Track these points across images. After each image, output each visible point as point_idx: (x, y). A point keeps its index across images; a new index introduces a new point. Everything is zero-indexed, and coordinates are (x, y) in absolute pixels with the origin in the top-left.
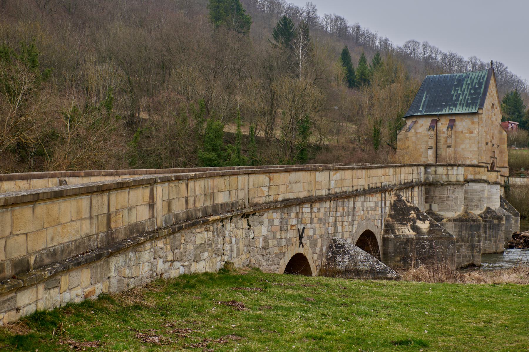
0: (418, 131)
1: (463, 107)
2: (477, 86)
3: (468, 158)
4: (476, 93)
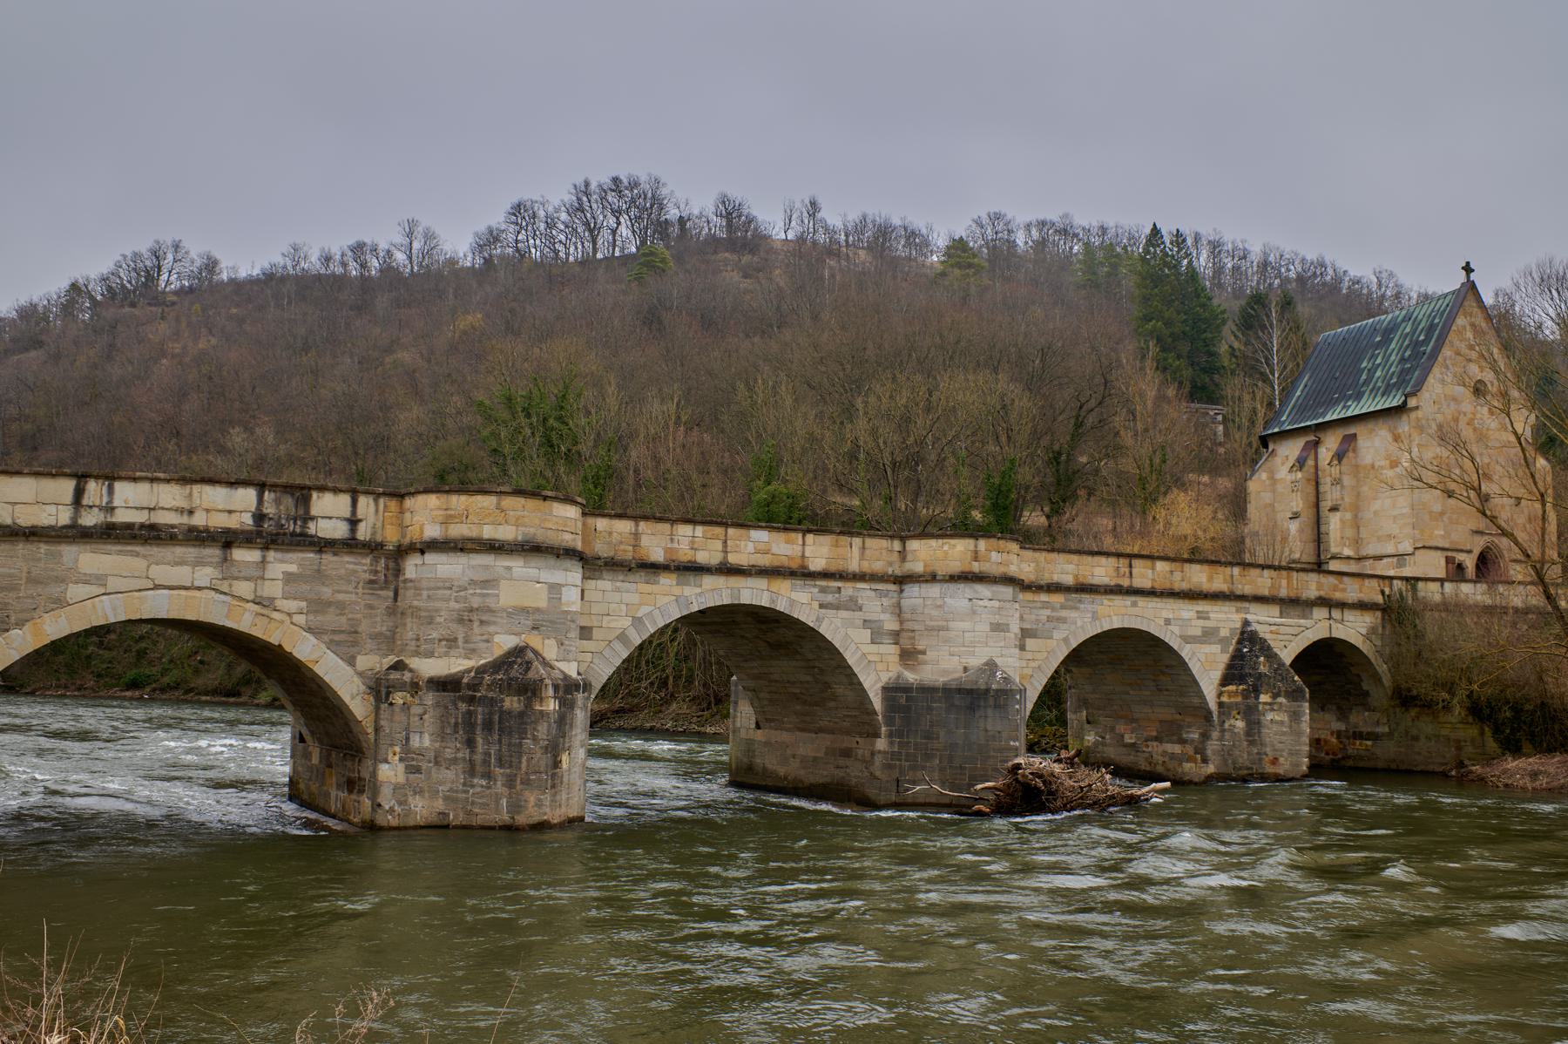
3: (1390, 536)
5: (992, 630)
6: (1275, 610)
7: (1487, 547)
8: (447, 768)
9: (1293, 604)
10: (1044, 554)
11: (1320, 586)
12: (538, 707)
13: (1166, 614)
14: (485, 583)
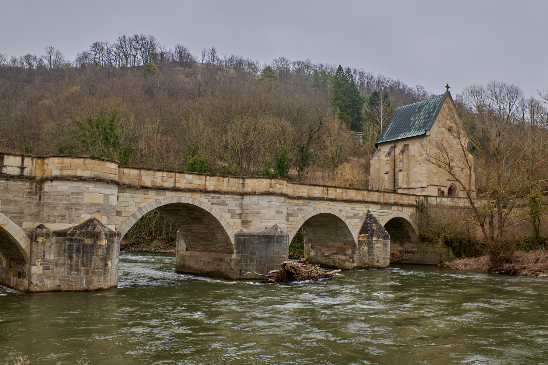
5: (277, 213)
6: (379, 207)
7: (452, 185)
8: (61, 268)
9: (385, 205)
10: (296, 185)
11: (395, 198)
12: (99, 243)
13: (340, 208)
14: (78, 194)
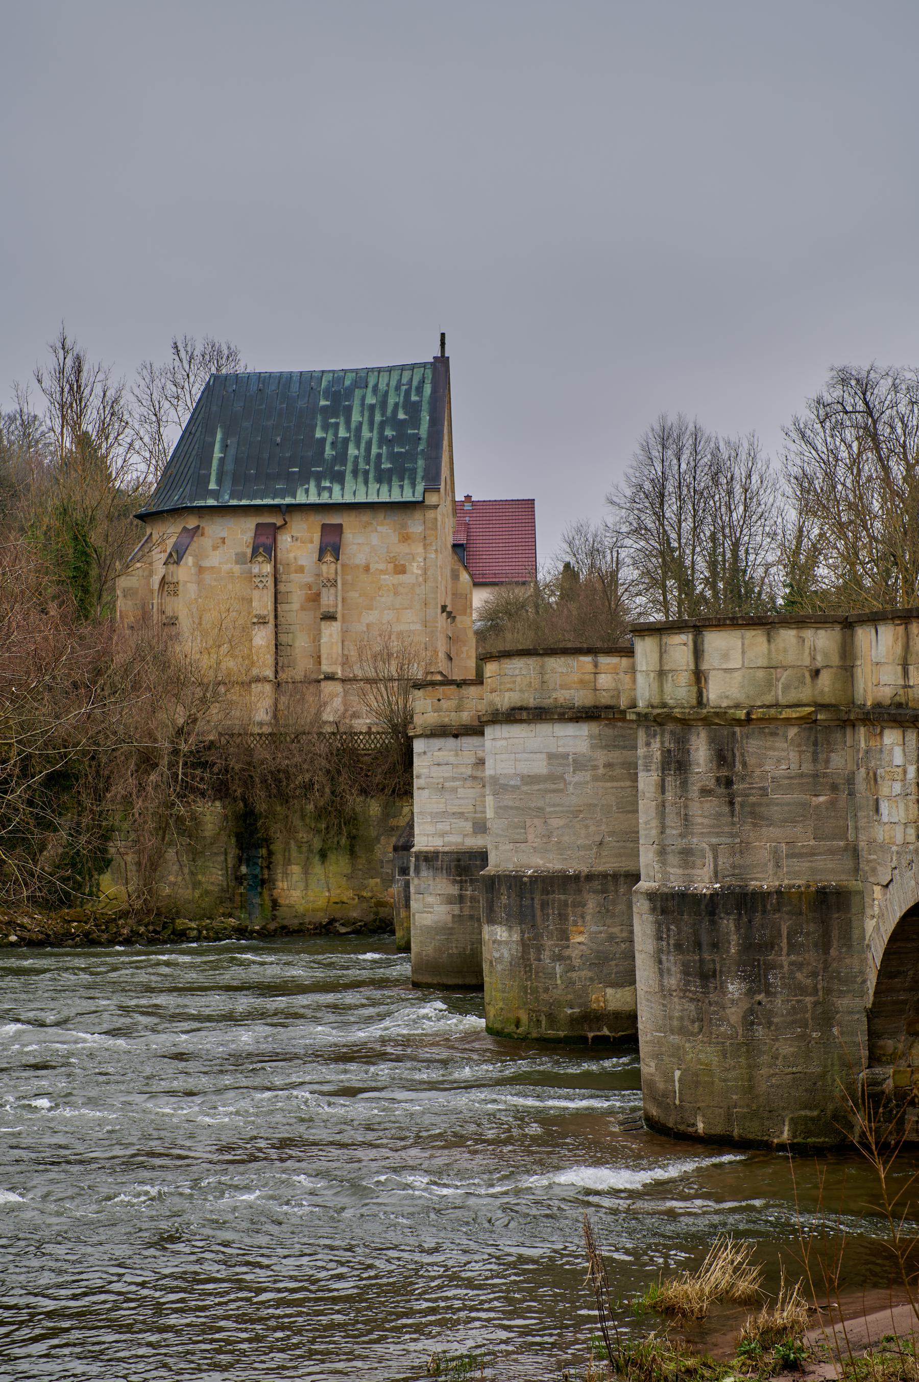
0: (206, 563)
1: (366, 482)
2: (401, 416)
4: (401, 438)
